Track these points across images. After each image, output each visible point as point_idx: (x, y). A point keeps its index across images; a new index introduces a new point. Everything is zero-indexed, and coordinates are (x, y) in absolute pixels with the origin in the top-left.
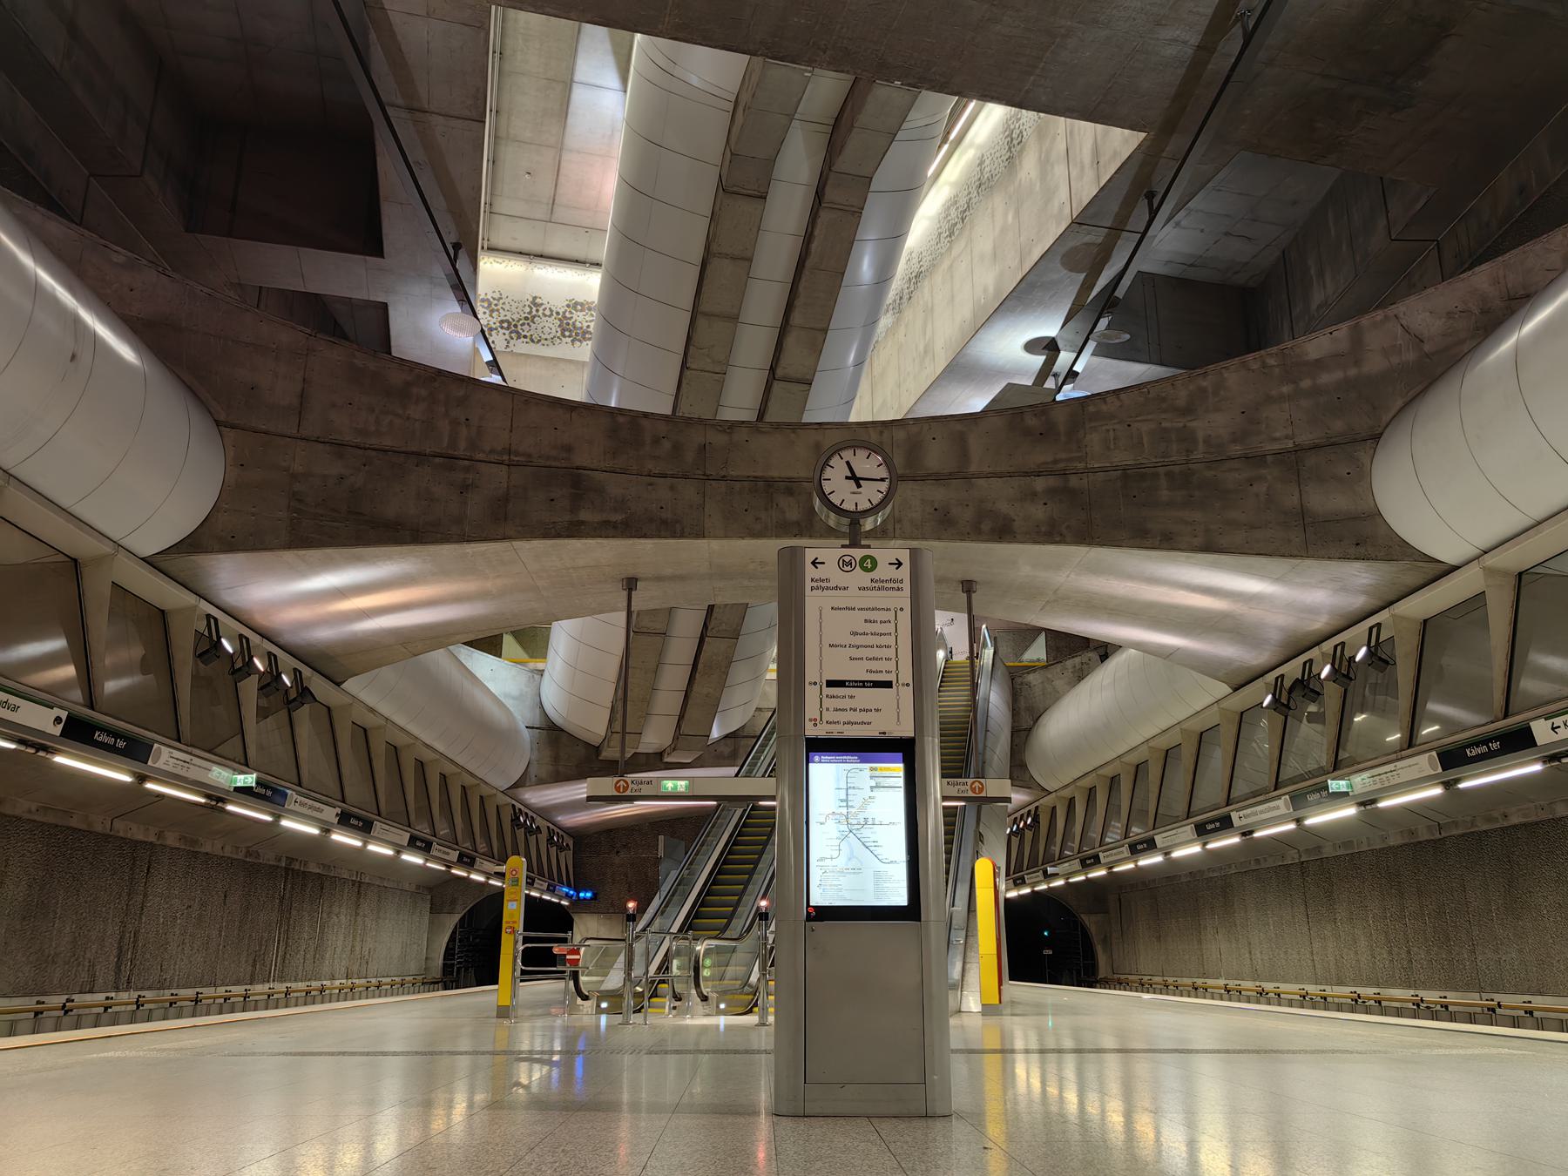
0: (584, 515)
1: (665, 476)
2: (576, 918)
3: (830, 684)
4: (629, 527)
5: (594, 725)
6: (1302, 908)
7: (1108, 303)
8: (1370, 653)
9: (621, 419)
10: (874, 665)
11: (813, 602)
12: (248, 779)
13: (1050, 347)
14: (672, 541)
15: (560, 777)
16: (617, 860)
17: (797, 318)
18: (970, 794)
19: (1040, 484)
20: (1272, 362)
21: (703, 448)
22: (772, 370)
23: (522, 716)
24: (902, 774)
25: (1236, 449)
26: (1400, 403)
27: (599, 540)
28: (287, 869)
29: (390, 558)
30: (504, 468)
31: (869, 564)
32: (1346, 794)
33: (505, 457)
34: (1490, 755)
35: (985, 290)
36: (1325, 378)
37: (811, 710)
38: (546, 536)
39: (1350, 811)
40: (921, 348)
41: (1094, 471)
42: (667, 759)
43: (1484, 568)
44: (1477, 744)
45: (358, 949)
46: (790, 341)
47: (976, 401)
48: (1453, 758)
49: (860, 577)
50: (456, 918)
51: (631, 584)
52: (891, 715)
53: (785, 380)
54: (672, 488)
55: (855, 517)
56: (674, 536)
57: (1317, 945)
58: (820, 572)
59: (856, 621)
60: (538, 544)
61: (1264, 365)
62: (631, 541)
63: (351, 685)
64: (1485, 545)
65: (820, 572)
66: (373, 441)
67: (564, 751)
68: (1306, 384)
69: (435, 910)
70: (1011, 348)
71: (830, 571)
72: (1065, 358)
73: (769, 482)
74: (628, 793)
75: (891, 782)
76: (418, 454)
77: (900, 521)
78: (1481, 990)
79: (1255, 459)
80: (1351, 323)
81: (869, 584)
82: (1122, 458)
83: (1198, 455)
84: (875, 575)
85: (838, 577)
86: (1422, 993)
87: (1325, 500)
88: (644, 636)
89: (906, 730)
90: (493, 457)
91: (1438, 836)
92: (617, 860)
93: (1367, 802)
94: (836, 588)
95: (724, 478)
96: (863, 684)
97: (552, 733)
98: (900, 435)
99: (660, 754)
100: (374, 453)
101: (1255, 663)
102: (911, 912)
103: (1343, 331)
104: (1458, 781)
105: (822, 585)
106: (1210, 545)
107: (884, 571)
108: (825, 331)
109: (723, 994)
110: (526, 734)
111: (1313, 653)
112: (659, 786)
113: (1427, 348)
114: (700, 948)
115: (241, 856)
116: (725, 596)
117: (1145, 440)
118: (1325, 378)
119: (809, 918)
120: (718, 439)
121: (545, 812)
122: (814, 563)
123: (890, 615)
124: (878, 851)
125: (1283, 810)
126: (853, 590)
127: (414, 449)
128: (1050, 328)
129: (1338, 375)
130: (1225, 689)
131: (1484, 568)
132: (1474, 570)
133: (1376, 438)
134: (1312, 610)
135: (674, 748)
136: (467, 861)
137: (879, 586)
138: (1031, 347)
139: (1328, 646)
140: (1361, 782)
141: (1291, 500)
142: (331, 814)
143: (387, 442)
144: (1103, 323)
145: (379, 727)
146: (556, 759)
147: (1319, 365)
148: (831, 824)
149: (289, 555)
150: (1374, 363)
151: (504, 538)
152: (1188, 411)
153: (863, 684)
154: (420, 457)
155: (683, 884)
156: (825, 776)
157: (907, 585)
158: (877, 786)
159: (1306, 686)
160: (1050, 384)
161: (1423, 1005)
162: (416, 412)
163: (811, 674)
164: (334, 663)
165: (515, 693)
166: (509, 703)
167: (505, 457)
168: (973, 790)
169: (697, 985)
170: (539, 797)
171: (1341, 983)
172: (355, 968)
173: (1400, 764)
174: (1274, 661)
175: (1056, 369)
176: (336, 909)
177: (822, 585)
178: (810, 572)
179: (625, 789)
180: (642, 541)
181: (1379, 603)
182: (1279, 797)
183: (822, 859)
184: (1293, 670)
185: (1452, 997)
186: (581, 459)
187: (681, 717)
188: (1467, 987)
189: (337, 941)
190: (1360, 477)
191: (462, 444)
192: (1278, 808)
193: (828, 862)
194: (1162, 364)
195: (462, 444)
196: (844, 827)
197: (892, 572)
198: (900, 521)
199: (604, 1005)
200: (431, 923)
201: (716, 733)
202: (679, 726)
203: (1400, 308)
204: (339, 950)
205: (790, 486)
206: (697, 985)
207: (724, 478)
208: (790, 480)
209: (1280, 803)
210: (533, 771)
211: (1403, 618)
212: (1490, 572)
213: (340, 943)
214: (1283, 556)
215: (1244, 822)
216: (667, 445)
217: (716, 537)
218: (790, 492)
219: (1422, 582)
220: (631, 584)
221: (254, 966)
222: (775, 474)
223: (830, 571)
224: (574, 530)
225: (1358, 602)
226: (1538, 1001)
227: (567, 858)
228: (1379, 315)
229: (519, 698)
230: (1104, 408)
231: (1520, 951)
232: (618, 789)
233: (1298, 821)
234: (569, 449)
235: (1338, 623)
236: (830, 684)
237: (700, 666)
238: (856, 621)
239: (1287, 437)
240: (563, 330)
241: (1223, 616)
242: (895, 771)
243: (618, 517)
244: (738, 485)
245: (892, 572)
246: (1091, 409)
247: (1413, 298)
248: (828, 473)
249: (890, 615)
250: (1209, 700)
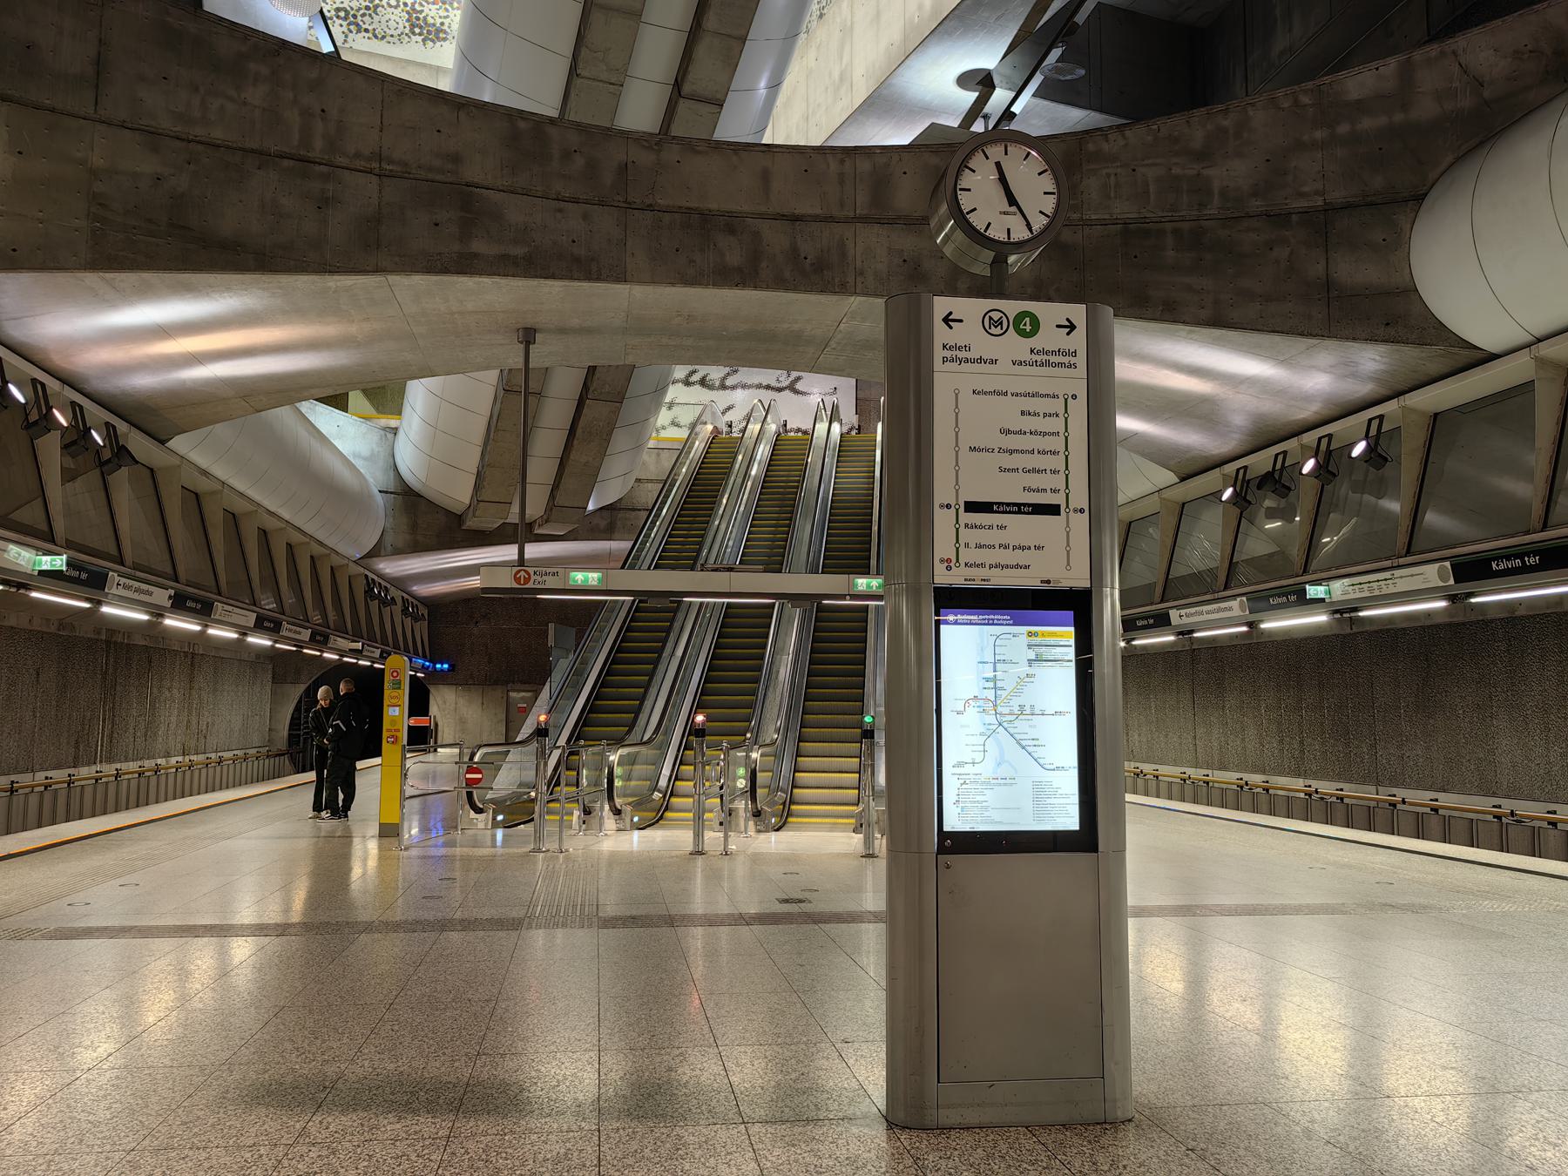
0: (478, 246)
1: (576, 201)
2: (432, 690)
3: (972, 507)
4: (534, 264)
5: (458, 492)
6: (1188, 695)
7: (1063, 29)
8: (1370, 450)
9: (522, 125)
10: (1035, 481)
11: (946, 382)
12: (58, 562)
13: (983, 82)
14: (586, 285)
15: (417, 547)
16: (476, 630)
17: (711, 21)
20: (1305, 100)
21: (624, 168)
22: (678, 85)
23: (375, 478)
24: (1072, 642)
25: (1256, 205)
26: (1450, 159)
27: (497, 279)
28: (108, 642)
29: (228, 288)
30: (375, 179)
31: (1027, 326)
32: (1323, 600)
33: (375, 165)
34: (1525, 570)
35: (920, 7)
36: (1367, 123)
37: (943, 546)
38: (429, 270)
39: (1321, 618)
40: (836, 75)
41: (1089, 224)
42: (538, 531)
43: (1536, 358)
44: (1508, 558)
45: (194, 722)
46: (701, 51)
47: (902, 136)
48: (1472, 570)
49: (1013, 345)
51: (528, 336)
52: (1056, 553)
53: (692, 98)
54: (585, 217)
56: (589, 277)
57: (1200, 731)
58: (956, 335)
59: (1008, 412)
60: (419, 281)
61: (1296, 102)
62: (534, 282)
63: (178, 443)
64: (1539, 331)
65: (956, 335)
66: (199, 131)
67: (423, 519)
68: (1343, 128)
69: (278, 679)
70: (939, 84)
71: (970, 333)
72: (1000, 97)
73: (706, 217)
74: (530, 585)
75: (1057, 652)
76: (261, 153)
77: (862, 274)
78: (1378, 783)
79: (1278, 219)
80: (1402, 57)
81: (1028, 357)
82: (1123, 209)
83: (1211, 211)
84: (1037, 342)
85: (983, 344)
86: (1315, 784)
87: (1354, 270)
88: (520, 393)
89: (1077, 578)
90: (359, 164)
91: (1348, 631)
92: (476, 630)
93: (1345, 611)
94: (980, 360)
95: (650, 208)
96: (1018, 508)
97: (408, 498)
98: (864, 165)
100: (200, 148)
101: (1216, 452)
102: (1085, 840)
103: (1391, 66)
104: (1472, 595)
105: (959, 355)
106: (1218, 316)
107: (1049, 337)
108: (743, 39)
109: (638, 805)
110: (379, 498)
111: (1291, 445)
112: (567, 577)
113: (1486, 94)
114: (614, 758)
115: (53, 629)
116: (605, 352)
117: (1152, 189)
118: (1367, 123)
119: (942, 850)
120: (645, 158)
121: (400, 582)
122: (947, 320)
123: (1057, 405)
124: (1038, 752)
125: (1236, 612)
126: (1004, 365)
127: (255, 146)
128: (988, 55)
129: (1382, 120)
130: (1171, 478)
131: (1536, 358)
132: (1524, 358)
133: (1418, 199)
134: (1307, 398)
135: (546, 520)
136: (320, 640)
137: (1044, 359)
138: (964, 80)
139: (1310, 438)
140: (1339, 589)
141: (1316, 270)
142: (162, 597)
143: (218, 134)
144: (1056, 53)
145: (214, 493)
146: (414, 527)
147: (1362, 106)
148: (972, 713)
149: (91, 278)
150: (1425, 109)
151: (377, 270)
152: (1203, 156)
153: (1018, 508)
154: (264, 157)
155: (578, 675)
156: (965, 645)
157: (1081, 360)
158: (1039, 659)
159: (1278, 481)
160: (978, 127)
161: (1315, 796)
162: (256, 95)
163: (943, 490)
164: (156, 417)
166: (358, 463)
167: (375, 165)
169: (611, 798)
170: (392, 567)
171: (1223, 768)
172: (193, 743)
173: (1397, 573)
174: (1239, 450)
175: (987, 109)
176: (167, 683)
177: (959, 355)
178: (941, 334)
179: (527, 580)
180: (550, 282)
181: (1384, 392)
182: (1234, 597)
183: (960, 764)
184: (1261, 462)
185: (1349, 790)
186: (474, 171)
187: (556, 486)
188: (1364, 780)
189: (170, 716)
190: (1397, 245)
191: (318, 144)
192: (1230, 609)
193: (968, 769)
194: (1101, 110)
195: (318, 144)
196: (991, 719)
197: (1060, 340)
198: (862, 274)
199: (500, 818)
200: (274, 693)
201: (591, 507)
202: (552, 496)
203: (1460, 42)
204: (173, 726)
205: (731, 223)
206: (611, 798)
207: (650, 208)
208: (731, 215)
209: (1235, 604)
210: (389, 539)
211: (1413, 410)
212: (1541, 362)
213: (174, 719)
214: (1302, 334)
215: (1185, 620)
216: (579, 162)
217: (641, 282)
218: (731, 230)
219: (1446, 370)
220: (528, 336)
221: (77, 748)
222: (714, 206)
224: (465, 265)
225: (1364, 389)
226: (1446, 799)
227: (421, 629)
228: (1434, 50)
229: (371, 458)
230: (1105, 147)
231: (1428, 748)
232: (517, 580)
233: (1250, 624)
234: (456, 159)
235: (1327, 413)
236: (972, 507)
237: (579, 431)
238: (1008, 412)
239: (1317, 193)
240: (413, 26)
241: (1203, 400)
242: (1066, 635)
243: (519, 251)
244: (667, 218)
245: (1060, 340)
246: (1091, 147)
247: (1475, 30)
248: (967, 180)
249: (1057, 405)
250: (1147, 488)
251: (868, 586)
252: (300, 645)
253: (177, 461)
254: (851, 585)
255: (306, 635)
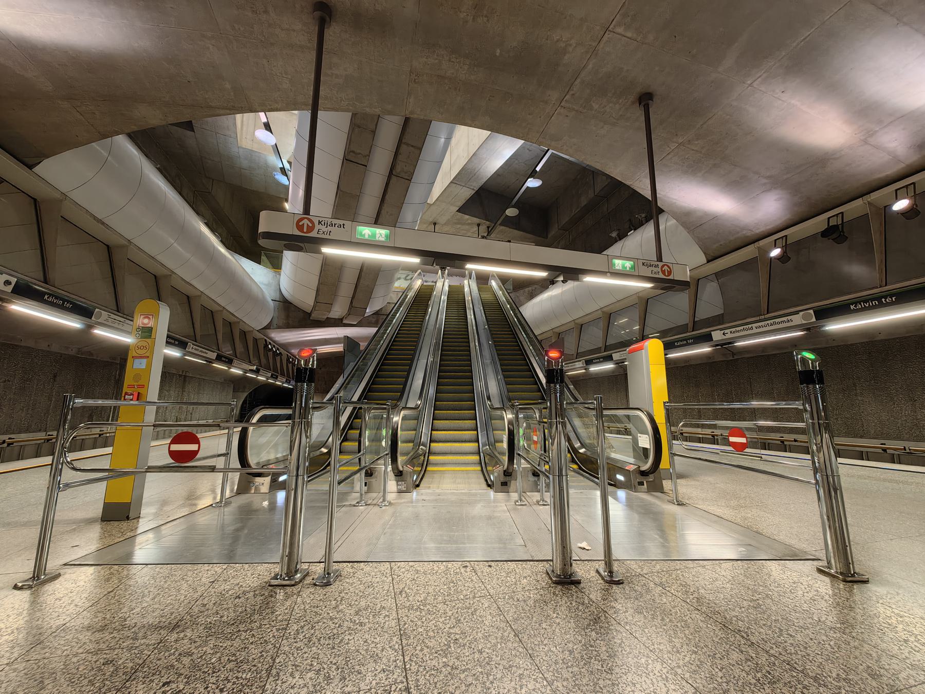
5: (306, 300)
18: (661, 276)
23: (269, 295)
42: (345, 322)
50: (245, 394)
67: (292, 314)
74: (313, 234)
99: (342, 320)
110: (271, 303)
112: (353, 230)
114: (397, 419)
121: (286, 346)
146: (288, 317)
165: (266, 282)
166: (262, 286)
168: (663, 272)
169: (394, 460)
172: (183, 417)
179: (311, 229)
182: (797, 313)
187: (353, 298)
202: (352, 302)
206: (394, 460)
210: (275, 322)
215: (729, 336)
229: (268, 285)
251: (623, 266)
252: (210, 361)
253: (58, 196)
254: (610, 264)
255: (213, 356)
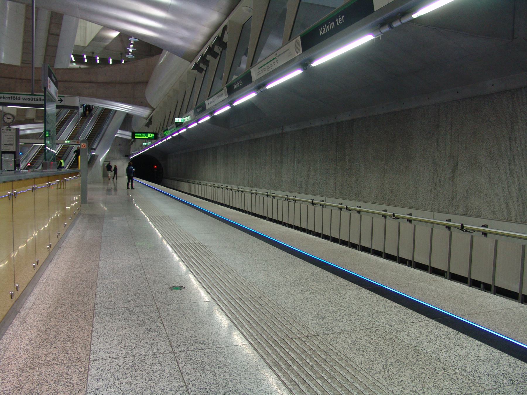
19: (88, 85)
37: (2, 148)
49: (9, 131)
55: (9, 123)
71: (5, 130)
85: (6, 131)
89: (14, 150)
99: (33, 119)
105: (4, 132)
137: (12, 133)
177: (4, 132)
223: (5, 130)
242: (13, 155)
